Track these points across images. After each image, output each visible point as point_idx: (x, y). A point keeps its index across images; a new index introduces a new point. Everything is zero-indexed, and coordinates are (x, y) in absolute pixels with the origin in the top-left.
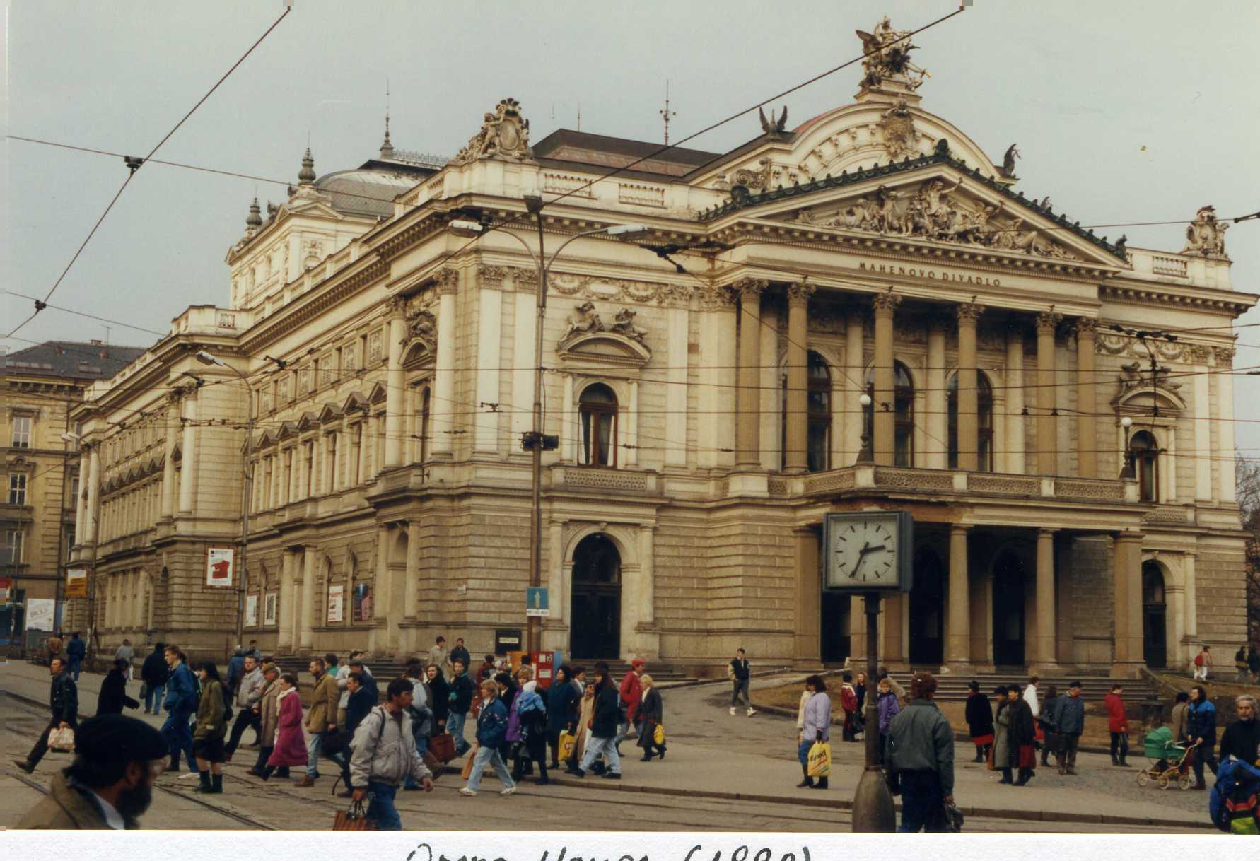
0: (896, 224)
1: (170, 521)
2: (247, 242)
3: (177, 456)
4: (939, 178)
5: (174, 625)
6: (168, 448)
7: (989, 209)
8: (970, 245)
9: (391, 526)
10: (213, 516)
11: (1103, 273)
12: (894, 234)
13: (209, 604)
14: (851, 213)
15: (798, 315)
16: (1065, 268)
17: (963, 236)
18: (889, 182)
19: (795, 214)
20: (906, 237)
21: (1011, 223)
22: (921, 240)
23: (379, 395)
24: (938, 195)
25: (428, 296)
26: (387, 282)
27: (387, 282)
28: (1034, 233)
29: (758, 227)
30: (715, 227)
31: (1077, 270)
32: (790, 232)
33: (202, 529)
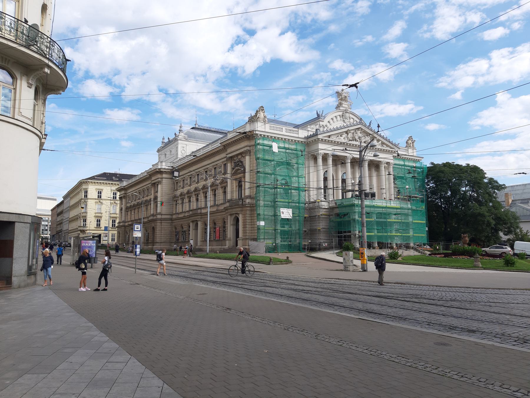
1: (153, 215)
2: (163, 147)
3: (156, 198)
4: (359, 128)
5: (157, 241)
6: (152, 197)
9: (231, 215)
10: (166, 214)
13: (165, 236)
15: (330, 161)
16: (387, 150)
18: (350, 128)
19: (329, 136)
21: (375, 139)
23: (224, 182)
24: (360, 132)
25: (240, 157)
26: (226, 153)
27: (226, 153)
29: (322, 139)
30: (310, 140)
31: (389, 151)
33: (163, 217)
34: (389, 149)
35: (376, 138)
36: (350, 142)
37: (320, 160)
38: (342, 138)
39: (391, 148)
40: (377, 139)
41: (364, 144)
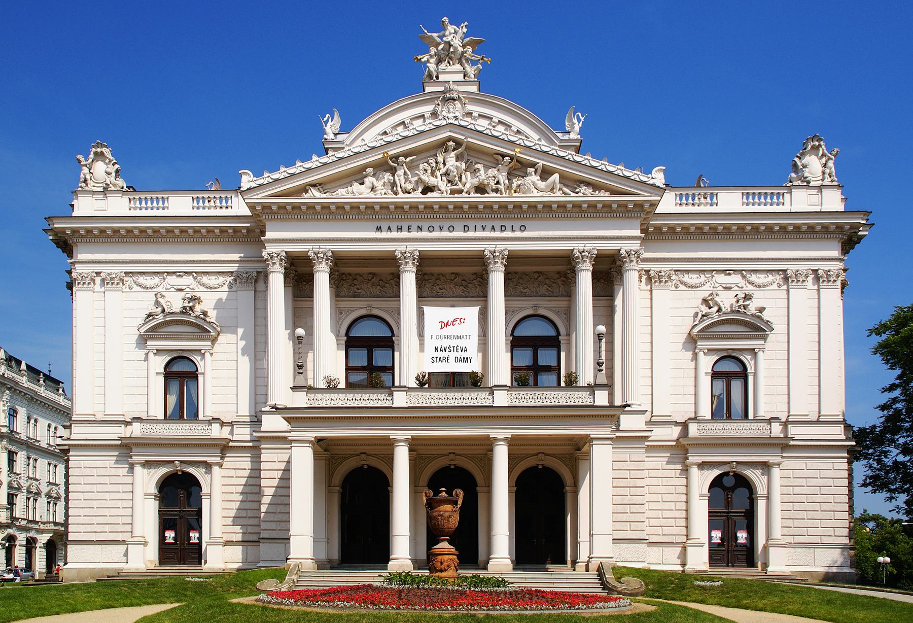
0: (409, 187)
8: (486, 195)
12: (407, 195)
14: (362, 184)
16: (592, 206)
17: (481, 189)
19: (304, 189)
20: (417, 197)
22: (432, 197)
28: (556, 177)
31: (607, 206)
34: (604, 196)
35: (533, 165)
36: (402, 198)
37: (277, 282)
39: (614, 192)
40: (539, 171)
41: (472, 194)
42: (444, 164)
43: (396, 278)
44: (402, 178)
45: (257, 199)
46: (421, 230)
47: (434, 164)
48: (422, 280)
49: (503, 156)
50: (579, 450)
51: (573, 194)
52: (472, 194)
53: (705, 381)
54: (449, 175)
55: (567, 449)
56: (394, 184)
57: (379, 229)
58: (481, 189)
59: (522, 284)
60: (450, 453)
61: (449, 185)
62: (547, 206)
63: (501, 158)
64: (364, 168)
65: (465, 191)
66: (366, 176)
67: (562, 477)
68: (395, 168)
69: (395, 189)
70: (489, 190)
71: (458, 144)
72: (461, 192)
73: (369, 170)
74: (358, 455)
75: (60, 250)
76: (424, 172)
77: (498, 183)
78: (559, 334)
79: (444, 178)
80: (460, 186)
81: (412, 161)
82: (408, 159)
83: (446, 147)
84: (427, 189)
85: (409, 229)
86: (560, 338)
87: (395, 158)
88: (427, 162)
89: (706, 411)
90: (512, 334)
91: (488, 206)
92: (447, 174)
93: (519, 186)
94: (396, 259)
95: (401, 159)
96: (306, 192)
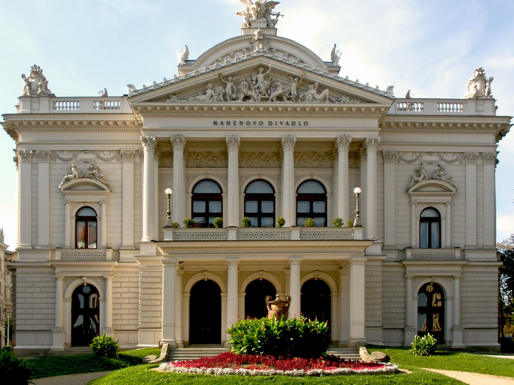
0: (234, 96)
4: (261, 66)
7: (296, 79)
8: (283, 102)
11: (378, 109)
14: (205, 94)
15: (178, 154)
16: (350, 109)
17: (280, 98)
19: (167, 97)
21: (312, 86)
31: (359, 109)
32: (164, 108)
35: (312, 83)
38: (203, 97)
40: (316, 86)
42: (257, 81)
43: (225, 155)
44: (230, 91)
45: (138, 103)
46: (242, 124)
47: (250, 82)
48: (241, 155)
49: (294, 77)
50: (341, 268)
51: (337, 102)
52: (274, 102)
53: (416, 222)
54: (260, 88)
55: (333, 268)
56: (224, 95)
57: (215, 123)
58: (280, 98)
59: (303, 160)
60: (260, 270)
61: (260, 95)
62: (322, 109)
63: (292, 78)
64: (207, 83)
65: (270, 99)
66: (207, 89)
67: (328, 285)
68: (226, 84)
69: (226, 97)
70: (285, 98)
71: (266, 68)
72: (267, 99)
73: (209, 85)
74: (202, 272)
75: (9, 136)
76: (245, 86)
77: (290, 94)
78: (326, 193)
79: (256, 90)
80: (267, 96)
81: (236, 80)
82: (234, 78)
83: (258, 71)
84: (247, 98)
85: (234, 123)
86: (327, 195)
87: (226, 77)
88: (246, 80)
89: (415, 242)
90: (297, 193)
91: (285, 109)
92: (258, 88)
93: (304, 96)
94: (225, 143)
95: (230, 78)
96: (169, 98)
